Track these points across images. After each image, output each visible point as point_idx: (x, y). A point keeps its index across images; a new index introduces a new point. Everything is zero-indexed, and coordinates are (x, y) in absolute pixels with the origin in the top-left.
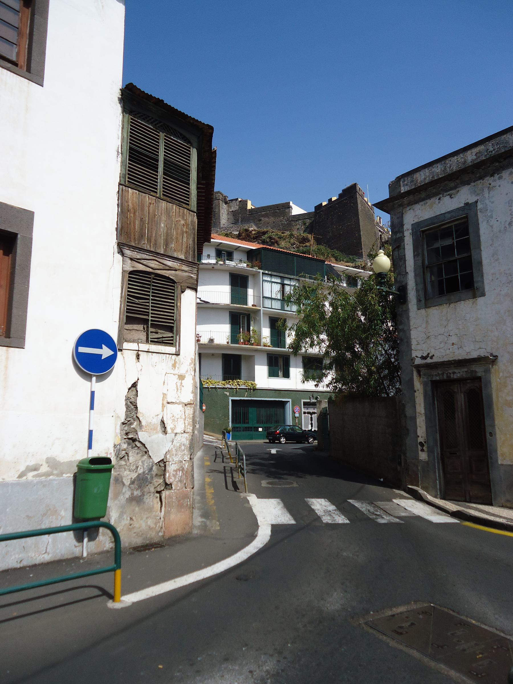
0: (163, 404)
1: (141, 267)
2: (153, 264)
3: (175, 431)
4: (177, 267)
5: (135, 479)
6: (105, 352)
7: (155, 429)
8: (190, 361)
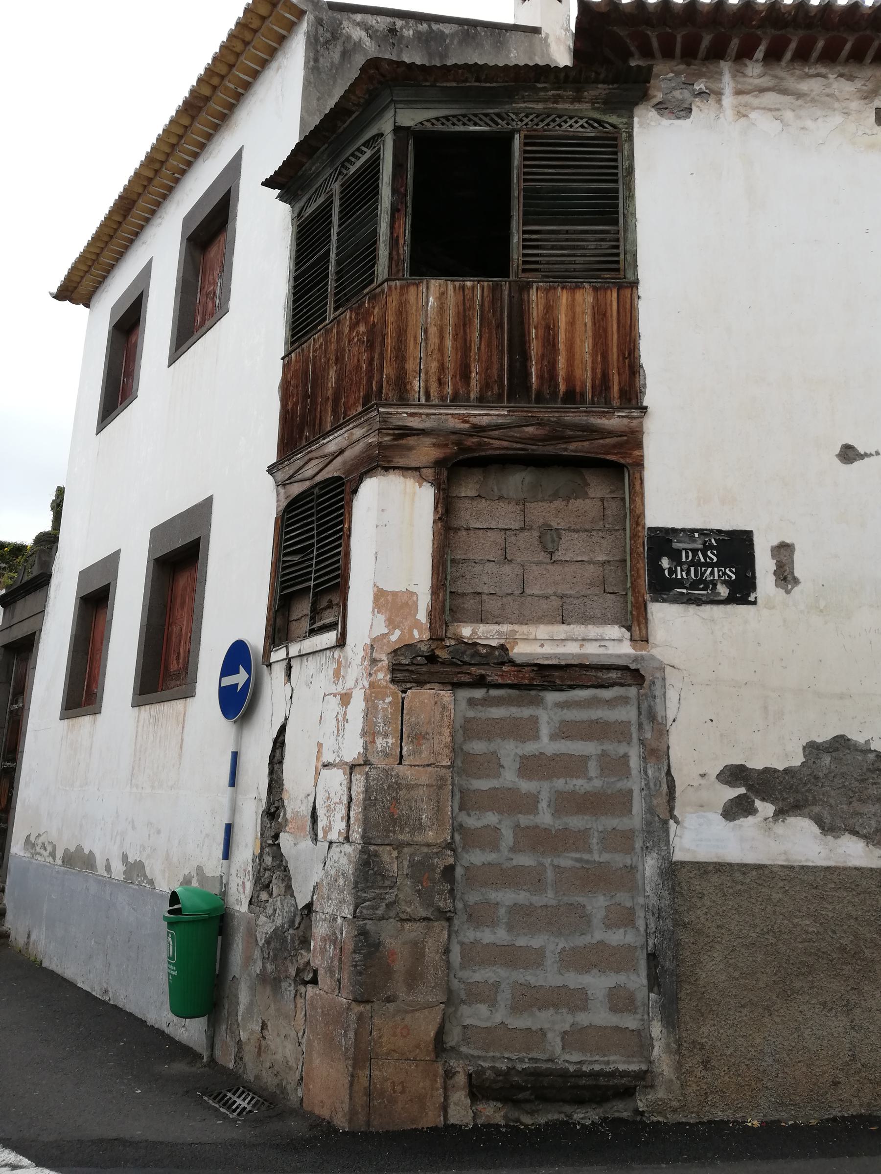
0: (316, 769)
1: (296, 489)
2: (309, 471)
3: (329, 838)
4: (345, 443)
5: (271, 937)
6: (240, 678)
7: (301, 828)
8: (362, 654)
